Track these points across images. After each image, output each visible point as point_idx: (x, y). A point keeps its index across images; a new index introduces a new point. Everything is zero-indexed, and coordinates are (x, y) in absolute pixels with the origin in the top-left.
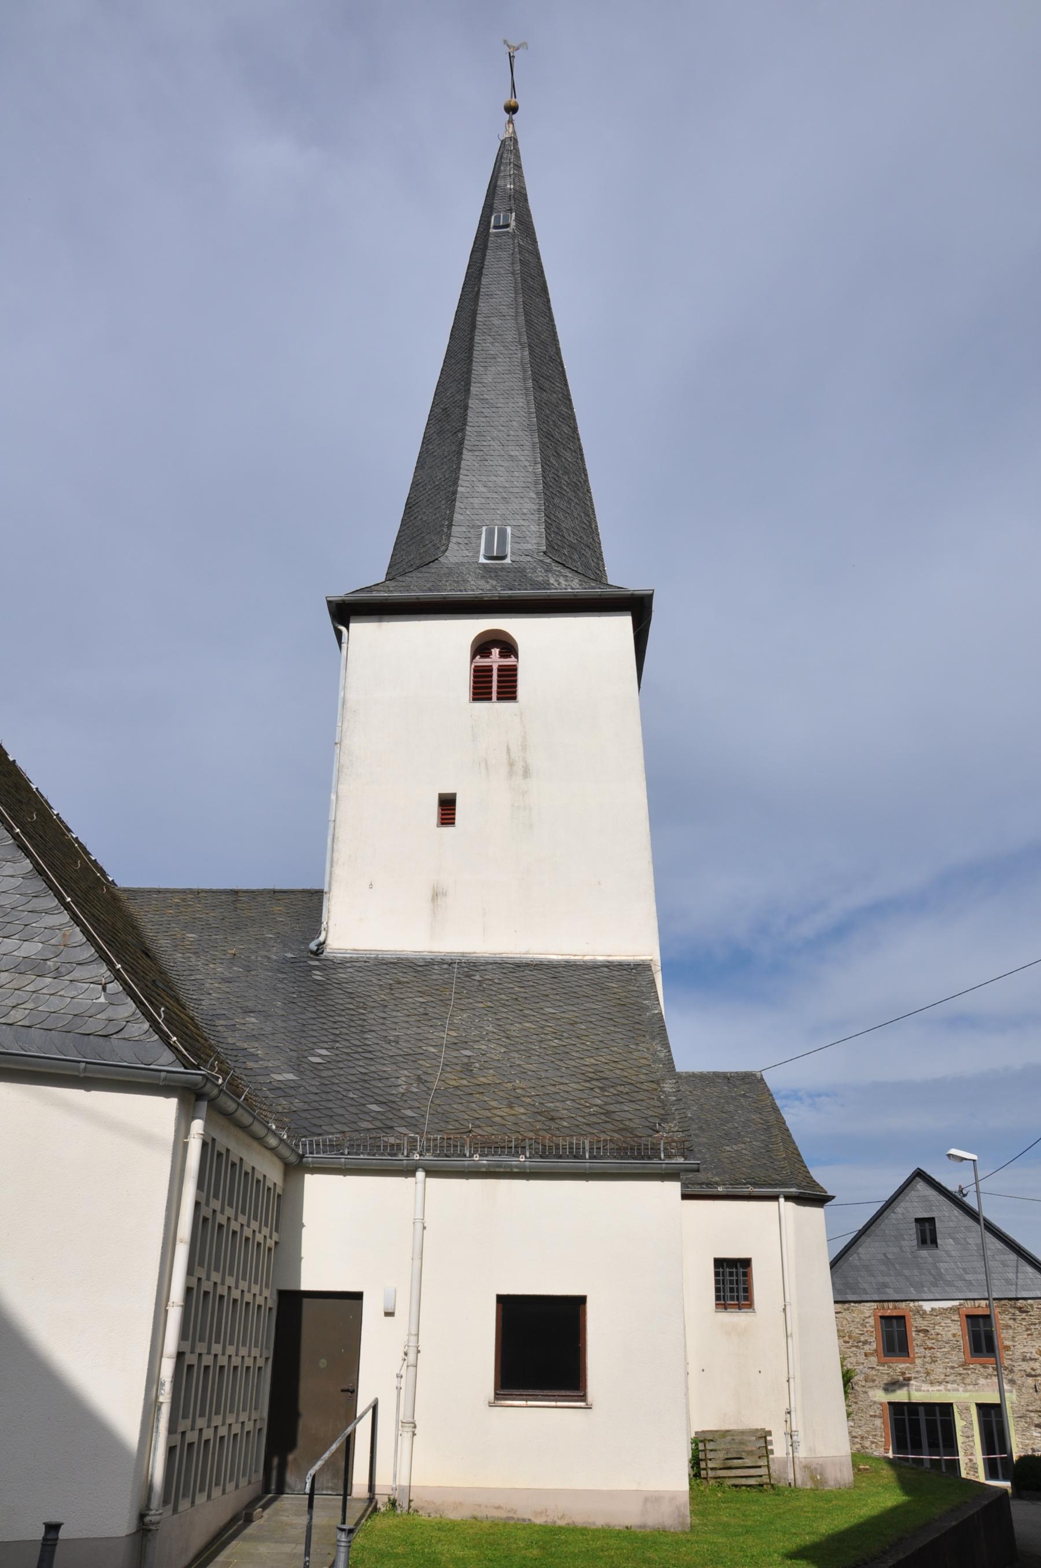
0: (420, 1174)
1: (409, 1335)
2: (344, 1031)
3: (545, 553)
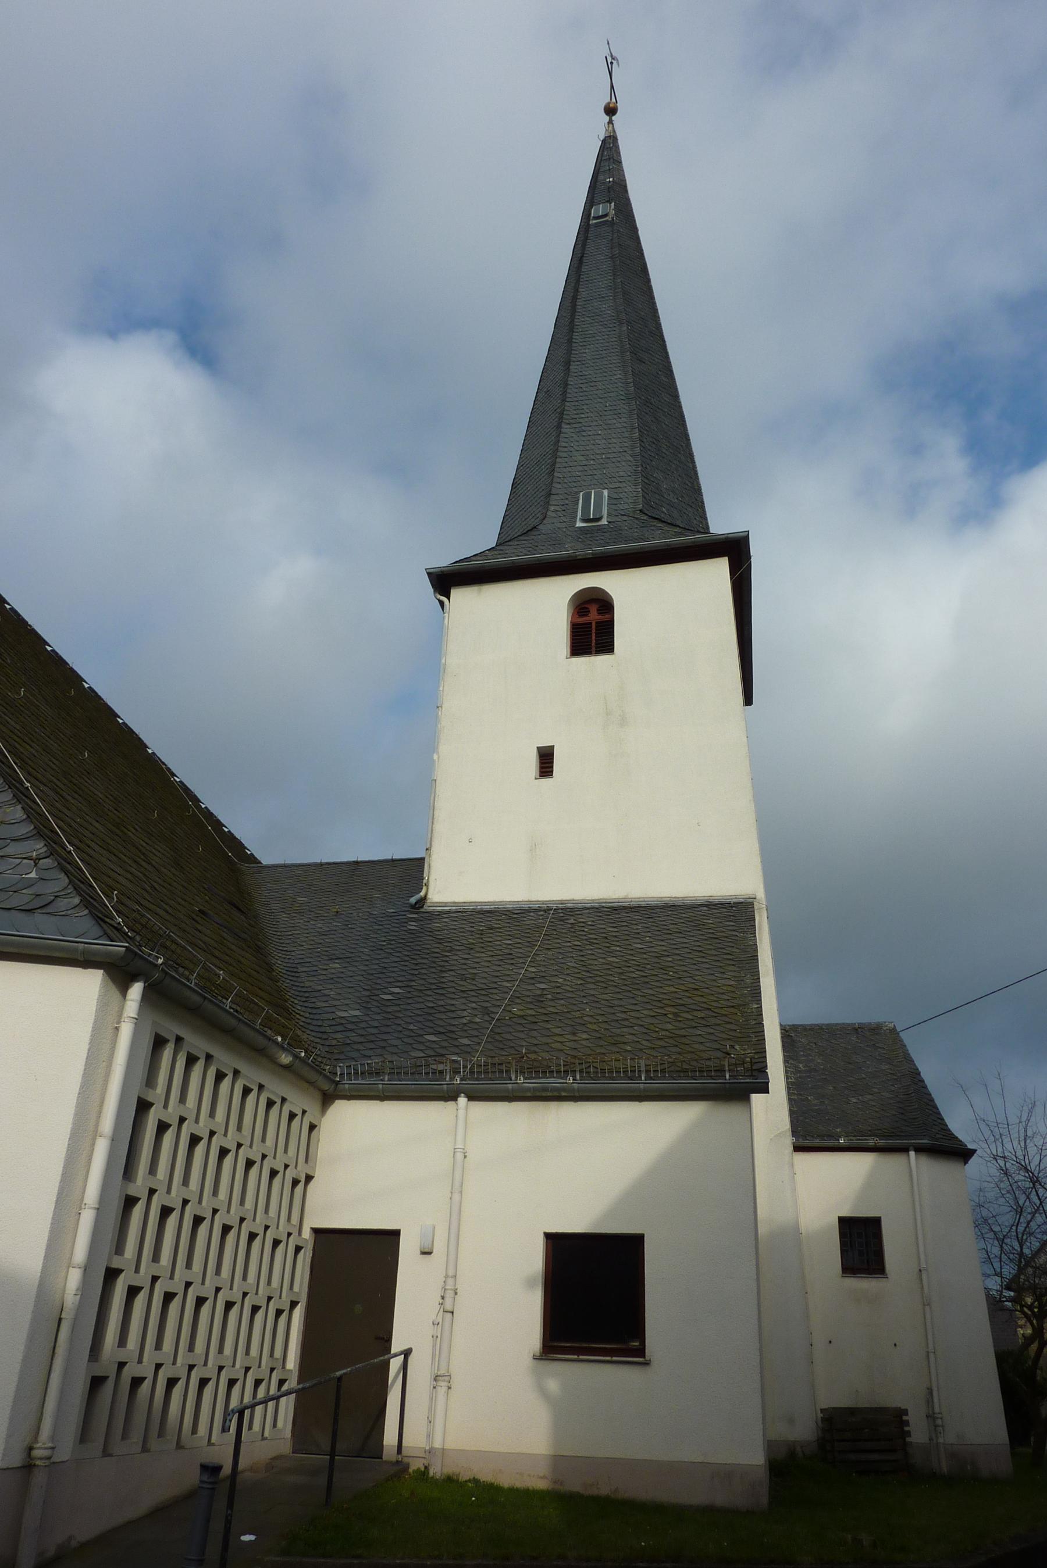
0: (462, 1100)
1: (447, 1276)
2: (423, 971)
3: (641, 511)
